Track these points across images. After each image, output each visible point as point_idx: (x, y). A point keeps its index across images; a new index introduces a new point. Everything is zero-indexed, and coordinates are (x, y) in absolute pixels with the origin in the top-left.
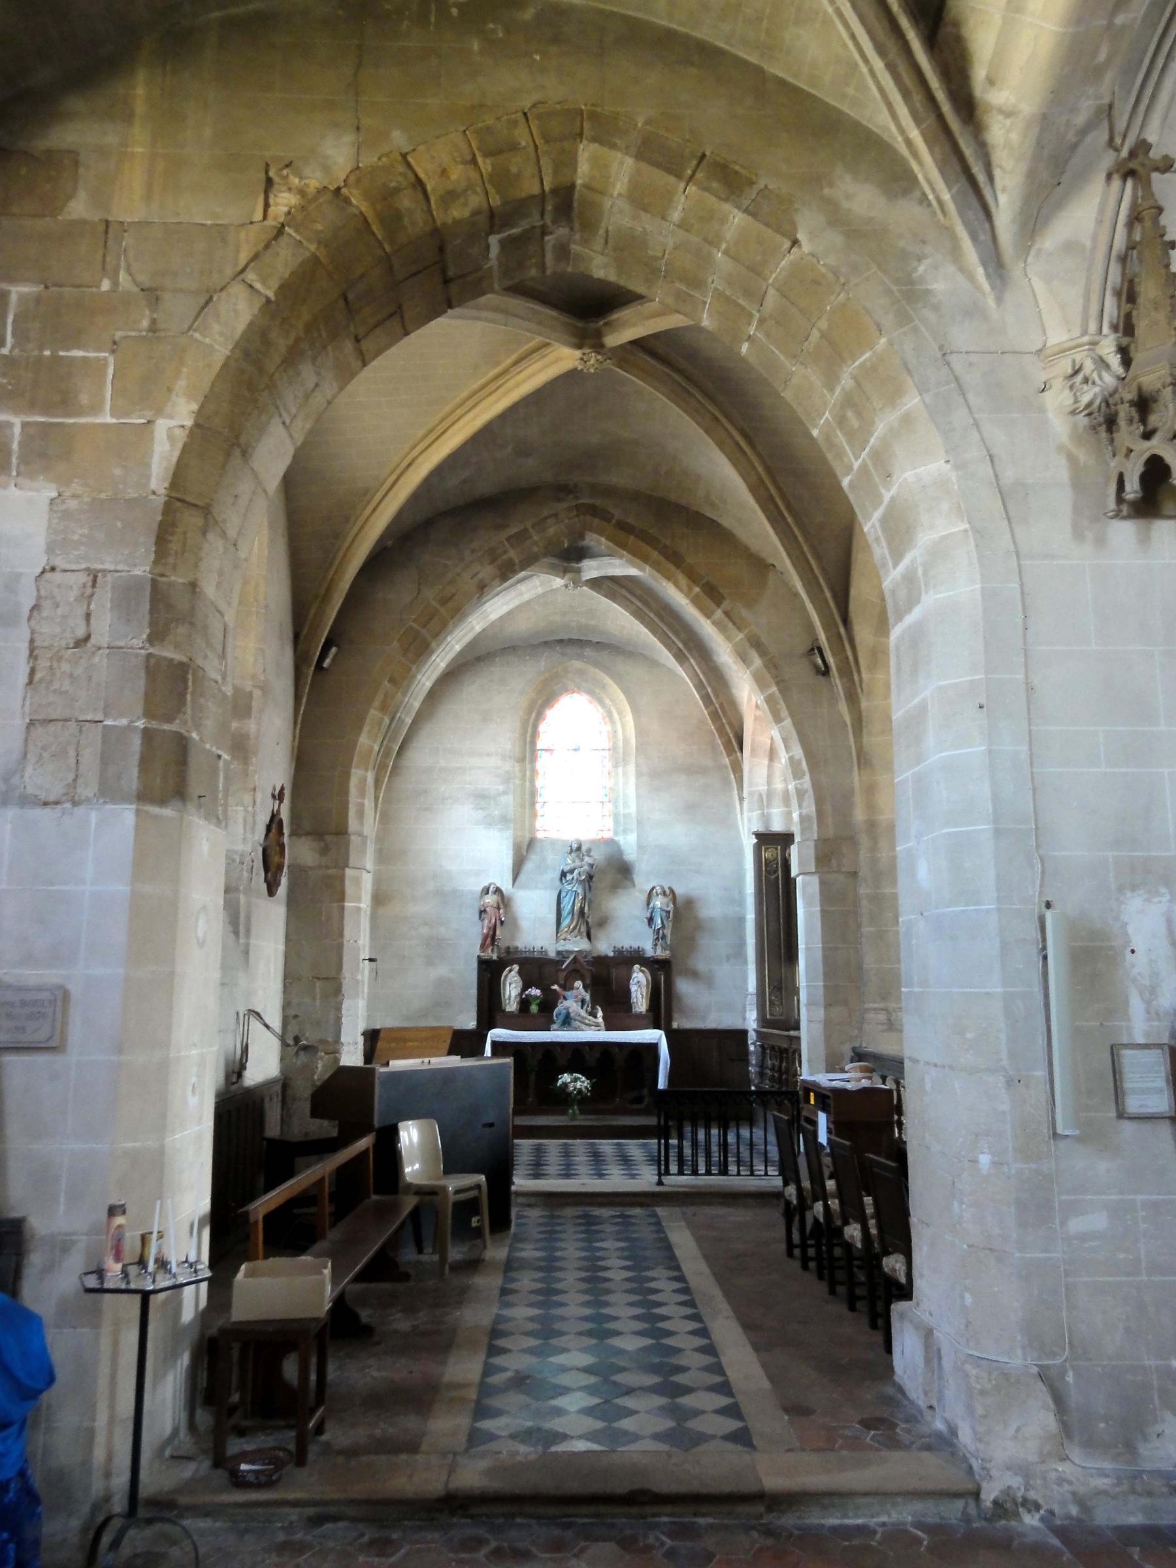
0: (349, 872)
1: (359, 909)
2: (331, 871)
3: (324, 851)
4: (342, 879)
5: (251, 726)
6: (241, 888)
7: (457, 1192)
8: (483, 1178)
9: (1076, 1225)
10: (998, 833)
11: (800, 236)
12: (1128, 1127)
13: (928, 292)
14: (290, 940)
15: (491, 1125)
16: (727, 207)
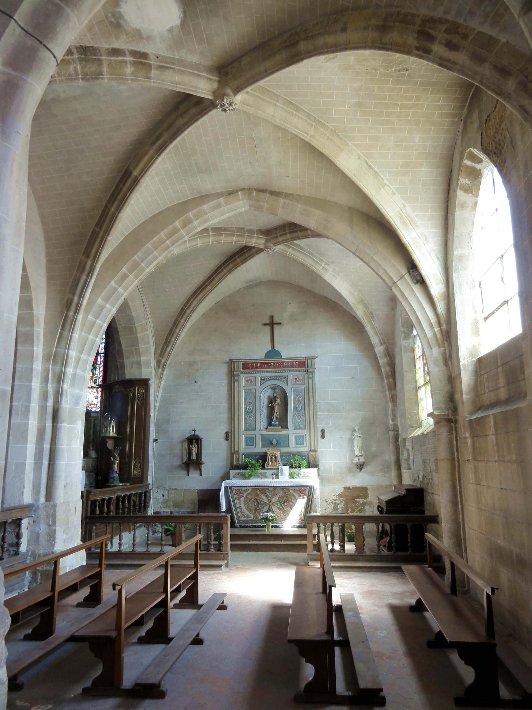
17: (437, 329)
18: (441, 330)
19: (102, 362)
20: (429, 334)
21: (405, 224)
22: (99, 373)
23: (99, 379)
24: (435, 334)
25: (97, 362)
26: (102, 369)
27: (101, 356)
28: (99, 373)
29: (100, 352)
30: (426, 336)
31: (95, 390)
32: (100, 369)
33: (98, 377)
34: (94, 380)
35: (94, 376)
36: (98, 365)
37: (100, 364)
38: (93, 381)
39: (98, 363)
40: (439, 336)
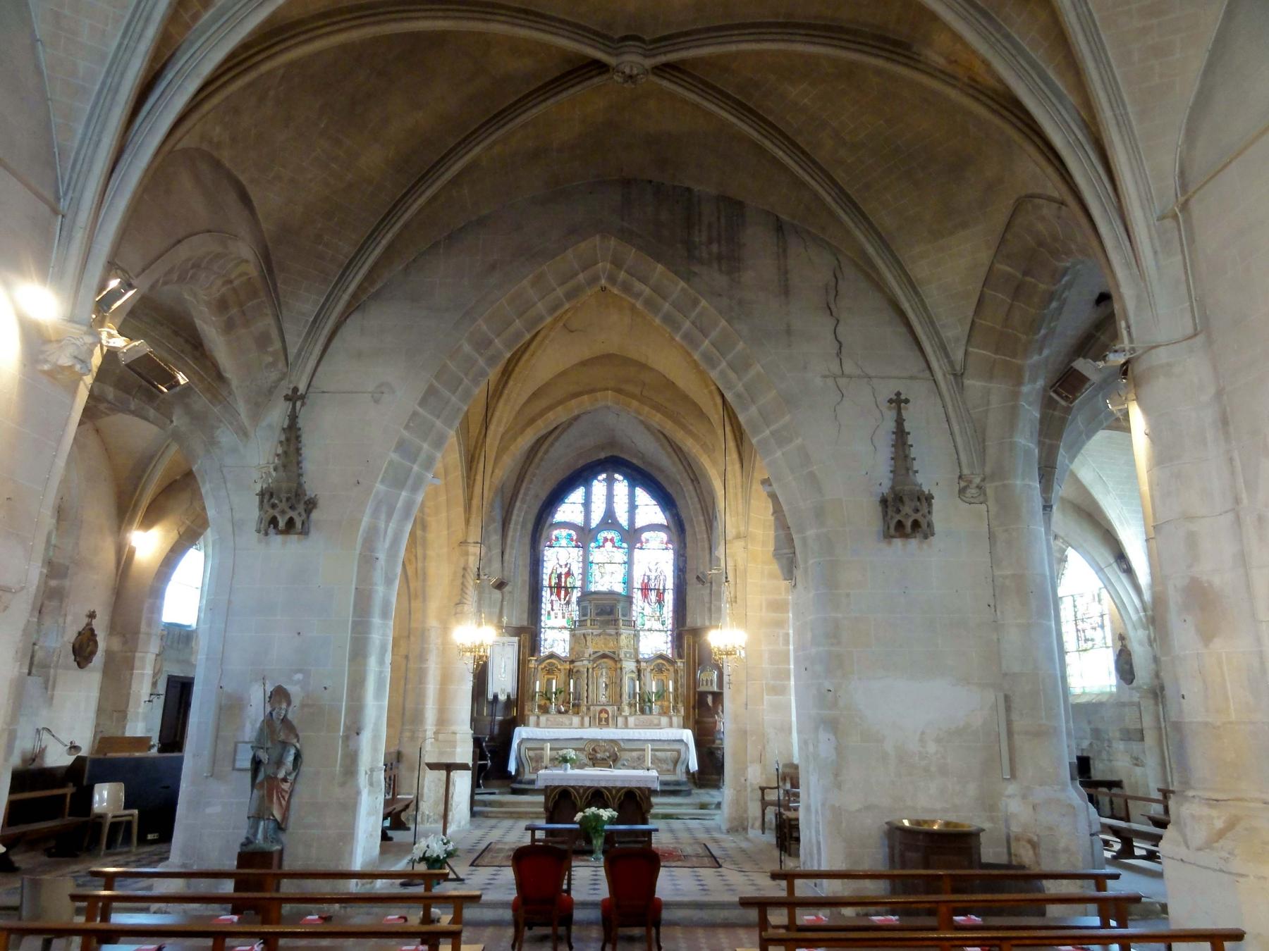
0: (138, 655)
1: (143, 675)
2: (129, 654)
3: (125, 643)
4: (134, 658)
5: (67, 583)
6: (52, 665)
7: (114, 817)
8: (136, 812)
9: (209, 810)
10: (207, 659)
11: (174, 419)
12: (236, 774)
13: (219, 442)
14: (102, 689)
15: (168, 787)
16: (147, 407)
17: (1142, 614)
18: (1146, 615)
20: (1134, 617)
21: (1122, 524)
24: (1140, 618)
30: (1130, 617)
31: (663, 633)
39: (666, 601)
40: (1144, 620)
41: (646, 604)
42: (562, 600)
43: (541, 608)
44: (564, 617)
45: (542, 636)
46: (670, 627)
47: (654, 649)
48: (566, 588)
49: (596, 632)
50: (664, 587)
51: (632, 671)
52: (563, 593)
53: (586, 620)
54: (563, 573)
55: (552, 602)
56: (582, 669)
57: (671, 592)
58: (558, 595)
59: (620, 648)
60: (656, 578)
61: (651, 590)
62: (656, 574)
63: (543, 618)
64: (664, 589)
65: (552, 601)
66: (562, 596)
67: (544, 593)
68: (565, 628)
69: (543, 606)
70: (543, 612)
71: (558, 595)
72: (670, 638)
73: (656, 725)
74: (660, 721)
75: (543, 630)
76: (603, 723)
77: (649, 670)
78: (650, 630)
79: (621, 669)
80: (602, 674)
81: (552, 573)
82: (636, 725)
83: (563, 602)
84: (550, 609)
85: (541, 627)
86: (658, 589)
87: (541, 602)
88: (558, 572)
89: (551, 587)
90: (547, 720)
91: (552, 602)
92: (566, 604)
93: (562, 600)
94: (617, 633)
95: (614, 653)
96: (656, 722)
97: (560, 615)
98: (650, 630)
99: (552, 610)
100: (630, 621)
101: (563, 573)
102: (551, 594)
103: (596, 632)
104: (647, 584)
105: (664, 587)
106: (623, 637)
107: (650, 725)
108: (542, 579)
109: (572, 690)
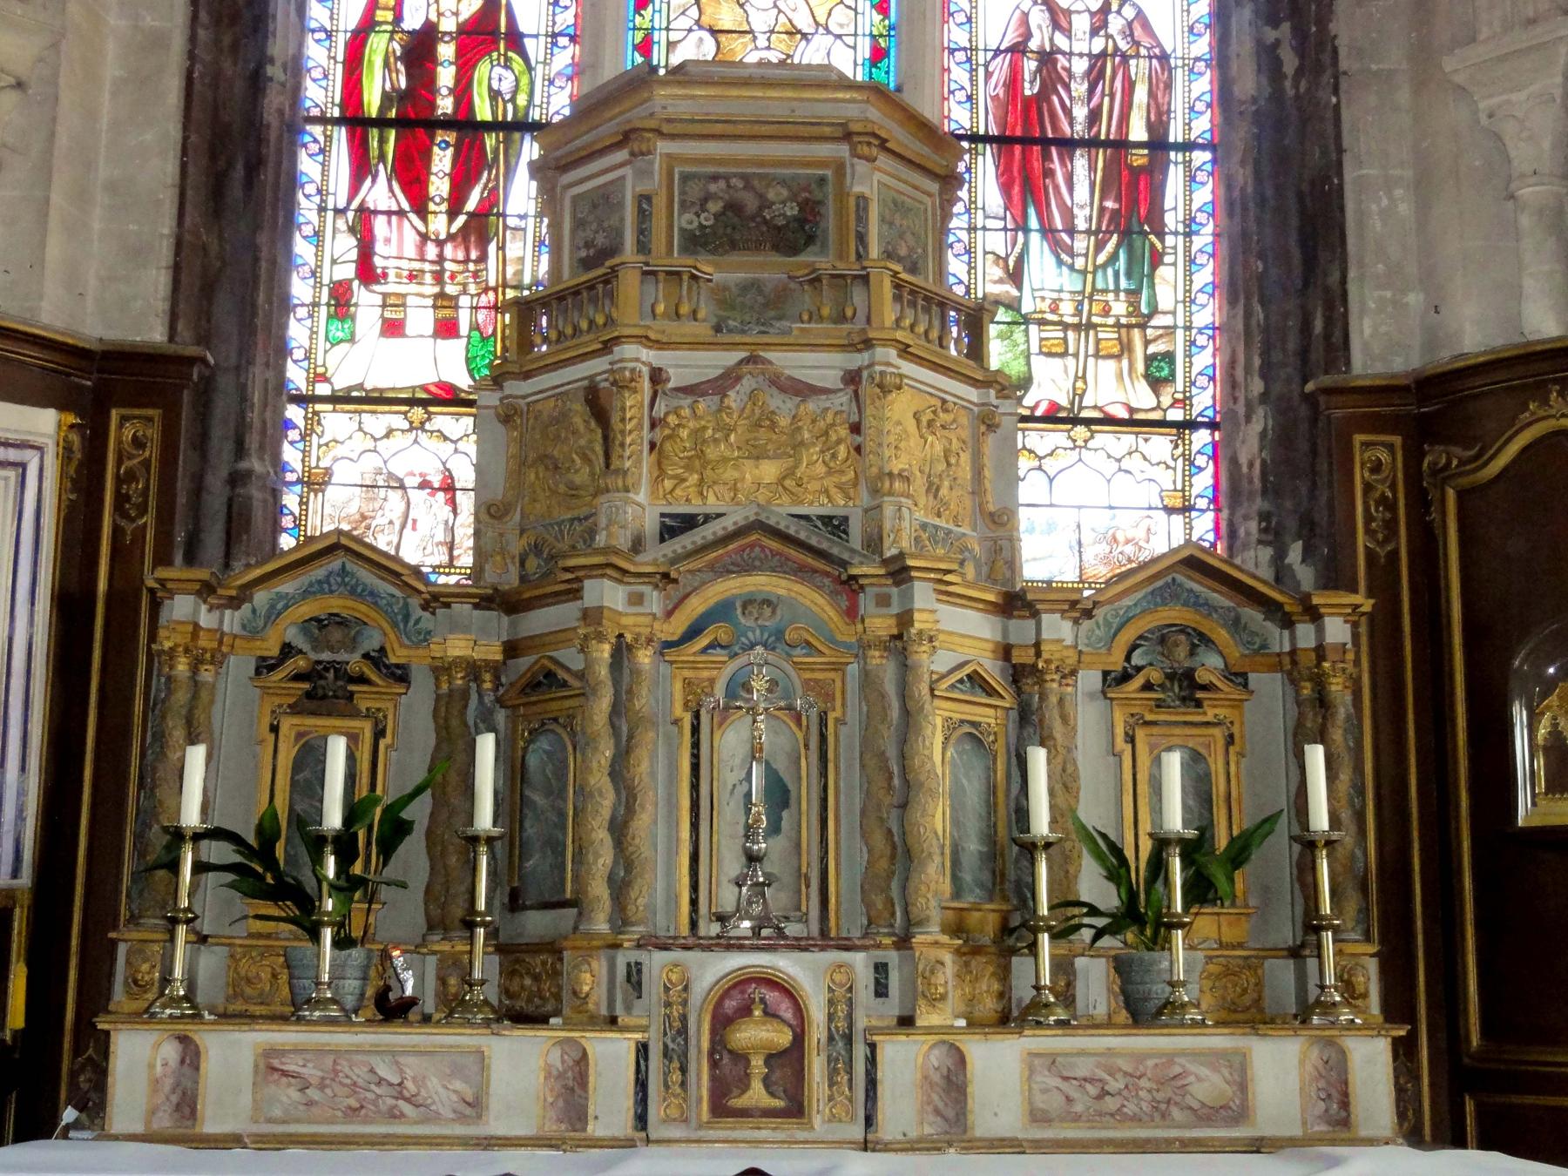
19: (1201, 218)
22: (1189, 301)
23: (1189, 355)
25: (1163, 212)
26: (1204, 275)
27: (1187, 164)
28: (1189, 301)
29: (1175, 134)
31: (1160, 445)
32: (1189, 275)
33: (1180, 333)
34: (1150, 359)
35: (1143, 327)
36: (1170, 240)
37: (1188, 235)
38: (1140, 367)
39: (1171, 220)
41: (1039, 251)
42: (439, 208)
43: (282, 264)
44: (447, 329)
45: (291, 455)
46: (1204, 401)
47: (1099, 549)
48: (465, 124)
49: (685, 367)
50: (1158, 127)
51: (976, 680)
52: (442, 161)
53: (609, 278)
54: (448, 25)
55: (364, 226)
56: (571, 658)
57: (1201, 157)
58: (412, 178)
59: (879, 484)
60: (1095, 76)
61: (1068, 145)
62: (1098, 45)
63: (297, 332)
64: (1158, 144)
65: (365, 216)
66: (439, 186)
67: (308, 165)
68: (447, 397)
69: (302, 248)
70: (300, 289)
71: (412, 178)
72: (1203, 482)
73: (1208, 1114)
74: (1243, 1087)
75: (294, 413)
76: (757, 1095)
77: (1090, 679)
78: (1052, 417)
79: (900, 642)
80: (739, 687)
81: (367, 25)
82: (1037, 1117)
83: (439, 224)
84: (347, 271)
85: (280, 391)
86: (1121, 145)
87: (286, 223)
88: (413, 21)
89: (354, 120)
90: (270, 1067)
91: (364, 226)
92: (462, 237)
93: (439, 208)
94: (852, 378)
95: (836, 526)
96: (1208, 1085)
97: (421, 319)
98: (1052, 417)
99: (367, 272)
100: (938, 303)
101: (448, 25)
102: (361, 168)
103: (685, 367)
104: (1035, 108)
105: (1158, 127)
106: (900, 407)
107: (1161, 1112)
108: (296, 68)
109: (485, 818)
